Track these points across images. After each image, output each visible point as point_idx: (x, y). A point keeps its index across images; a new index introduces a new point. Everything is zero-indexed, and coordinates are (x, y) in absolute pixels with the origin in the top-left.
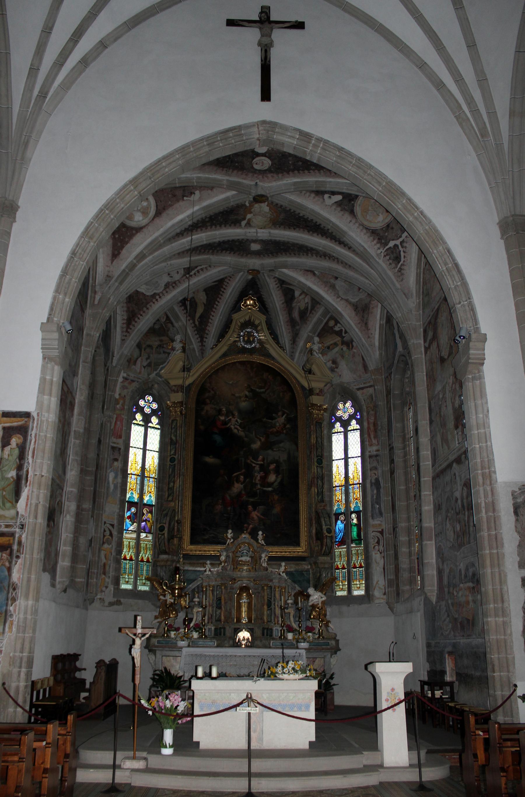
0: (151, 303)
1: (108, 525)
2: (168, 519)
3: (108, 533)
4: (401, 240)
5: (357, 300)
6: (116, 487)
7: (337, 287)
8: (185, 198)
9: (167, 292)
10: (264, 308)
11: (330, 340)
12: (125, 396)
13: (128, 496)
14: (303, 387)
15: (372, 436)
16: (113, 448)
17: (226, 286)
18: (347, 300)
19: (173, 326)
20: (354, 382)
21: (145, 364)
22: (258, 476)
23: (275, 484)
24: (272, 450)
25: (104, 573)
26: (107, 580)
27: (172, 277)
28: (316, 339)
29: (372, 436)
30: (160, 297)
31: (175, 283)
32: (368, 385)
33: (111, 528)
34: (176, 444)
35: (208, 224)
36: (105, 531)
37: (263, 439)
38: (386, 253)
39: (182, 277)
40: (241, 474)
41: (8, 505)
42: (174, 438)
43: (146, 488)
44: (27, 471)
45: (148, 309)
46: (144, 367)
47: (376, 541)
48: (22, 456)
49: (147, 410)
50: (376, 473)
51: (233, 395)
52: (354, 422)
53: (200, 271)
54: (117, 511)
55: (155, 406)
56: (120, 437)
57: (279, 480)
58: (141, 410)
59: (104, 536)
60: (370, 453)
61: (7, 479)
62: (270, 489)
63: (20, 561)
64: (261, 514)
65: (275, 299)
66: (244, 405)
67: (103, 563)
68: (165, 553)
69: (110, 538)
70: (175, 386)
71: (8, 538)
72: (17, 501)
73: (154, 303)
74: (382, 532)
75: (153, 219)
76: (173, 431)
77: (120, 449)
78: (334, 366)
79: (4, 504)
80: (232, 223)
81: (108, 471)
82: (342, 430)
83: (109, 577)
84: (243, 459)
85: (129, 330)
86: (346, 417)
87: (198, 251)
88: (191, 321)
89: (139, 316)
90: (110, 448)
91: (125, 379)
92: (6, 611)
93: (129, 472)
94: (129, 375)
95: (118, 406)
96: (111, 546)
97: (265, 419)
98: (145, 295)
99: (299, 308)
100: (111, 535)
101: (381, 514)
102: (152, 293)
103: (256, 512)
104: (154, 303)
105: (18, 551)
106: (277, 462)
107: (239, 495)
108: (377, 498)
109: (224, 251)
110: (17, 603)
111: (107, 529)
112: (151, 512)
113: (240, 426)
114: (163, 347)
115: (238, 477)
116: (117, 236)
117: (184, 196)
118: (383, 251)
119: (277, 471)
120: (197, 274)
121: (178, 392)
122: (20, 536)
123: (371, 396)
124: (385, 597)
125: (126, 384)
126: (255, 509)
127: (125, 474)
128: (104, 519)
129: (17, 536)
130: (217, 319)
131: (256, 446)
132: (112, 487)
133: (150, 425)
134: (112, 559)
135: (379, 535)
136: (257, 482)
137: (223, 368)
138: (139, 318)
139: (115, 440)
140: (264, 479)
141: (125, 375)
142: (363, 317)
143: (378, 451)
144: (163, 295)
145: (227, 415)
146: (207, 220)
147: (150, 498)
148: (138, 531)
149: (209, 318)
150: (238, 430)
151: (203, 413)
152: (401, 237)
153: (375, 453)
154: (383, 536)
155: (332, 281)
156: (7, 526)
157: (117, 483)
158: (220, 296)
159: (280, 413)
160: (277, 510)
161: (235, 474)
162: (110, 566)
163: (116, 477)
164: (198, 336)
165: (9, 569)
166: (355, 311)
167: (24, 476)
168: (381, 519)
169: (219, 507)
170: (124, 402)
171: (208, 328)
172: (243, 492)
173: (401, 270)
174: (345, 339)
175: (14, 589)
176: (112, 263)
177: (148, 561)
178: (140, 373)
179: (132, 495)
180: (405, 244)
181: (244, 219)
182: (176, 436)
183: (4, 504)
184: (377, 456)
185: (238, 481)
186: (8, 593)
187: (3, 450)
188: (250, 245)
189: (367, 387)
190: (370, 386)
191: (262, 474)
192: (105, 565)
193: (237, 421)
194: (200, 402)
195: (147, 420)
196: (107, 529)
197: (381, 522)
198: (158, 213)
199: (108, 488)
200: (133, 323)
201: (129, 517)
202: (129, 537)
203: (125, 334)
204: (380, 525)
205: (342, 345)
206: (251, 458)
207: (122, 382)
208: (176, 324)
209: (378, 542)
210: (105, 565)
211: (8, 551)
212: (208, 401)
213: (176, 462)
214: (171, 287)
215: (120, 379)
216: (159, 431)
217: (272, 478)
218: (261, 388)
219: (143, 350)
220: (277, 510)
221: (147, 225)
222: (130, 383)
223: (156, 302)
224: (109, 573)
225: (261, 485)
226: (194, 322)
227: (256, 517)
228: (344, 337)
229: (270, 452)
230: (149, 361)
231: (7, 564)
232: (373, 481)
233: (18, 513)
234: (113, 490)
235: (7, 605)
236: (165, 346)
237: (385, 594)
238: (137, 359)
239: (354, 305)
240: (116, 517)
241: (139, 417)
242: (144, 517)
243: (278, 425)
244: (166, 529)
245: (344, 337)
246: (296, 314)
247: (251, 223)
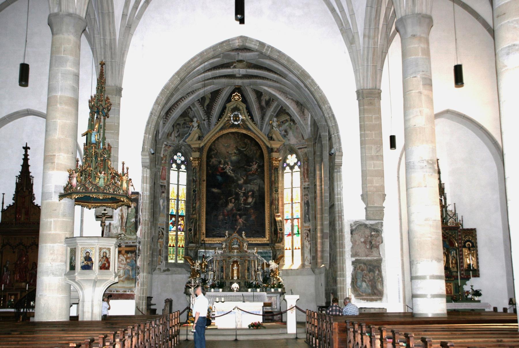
0: (180, 102)
1: (161, 229)
2: (193, 224)
3: (161, 233)
6: (164, 208)
10: (244, 100)
11: (284, 118)
13: (170, 211)
14: (267, 147)
15: (306, 176)
16: (162, 186)
19: (192, 110)
20: (296, 144)
21: (176, 135)
22: (242, 199)
23: (252, 203)
24: (250, 184)
25: (160, 255)
26: (162, 258)
28: (275, 119)
29: (306, 176)
30: (185, 99)
32: (304, 146)
33: (162, 230)
34: (196, 182)
36: (159, 232)
37: (245, 178)
40: (233, 198)
41: (133, 233)
42: (195, 178)
43: (180, 206)
44: (140, 219)
45: (178, 105)
46: (176, 137)
47: (306, 235)
48: (137, 212)
49: (179, 162)
51: (228, 152)
52: (296, 167)
54: (165, 220)
55: (183, 159)
56: (165, 179)
57: (254, 201)
58: (175, 161)
59: (159, 235)
61: (131, 222)
62: (249, 206)
63: (140, 257)
64: (245, 220)
65: (251, 97)
66: (234, 158)
68: (192, 243)
70: (194, 148)
71: (133, 248)
72: (136, 232)
74: (309, 230)
76: (194, 174)
77: (165, 186)
78: (285, 134)
79: (131, 233)
81: (160, 199)
82: (290, 171)
84: (234, 190)
85: (167, 118)
86: (292, 164)
91: (166, 145)
92: (136, 278)
93: (170, 198)
94: (168, 143)
95: (163, 162)
97: (246, 167)
99: (266, 100)
100: (163, 234)
101: (309, 220)
103: (241, 220)
105: (139, 253)
106: (253, 191)
107: (232, 210)
108: (307, 212)
110: (140, 274)
111: (160, 231)
112: (183, 220)
113: (232, 170)
114: (186, 124)
115: (231, 200)
119: (253, 196)
121: (196, 152)
122: (139, 247)
123: (306, 153)
124: (310, 265)
125: (167, 148)
126: (240, 217)
127: (168, 199)
128: (159, 226)
129: (138, 247)
130: (217, 108)
131: (241, 182)
132: (162, 207)
133: (180, 170)
135: (308, 232)
136: (242, 202)
137: (221, 136)
138: (173, 111)
139: (162, 181)
140: (245, 200)
141: (165, 143)
142: (301, 108)
143: (308, 185)
144: (186, 97)
145: (224, 165)
147: (182, 212)
148: (177, 230)
149: (213, 107)
150: (231, 173)
151: (211, 163)
153: (307, 186)
156: (133, 243)
159: (254, 163)
160: (253, 218)
161: (229, 198)
163: (164, 202)
164: (206, 116)
165: (136, 261)
166: (297, 105)
167: (139, 221)
169: (221, 217)
170: (166, 158)
171: (212, 112)
172: (234, 208)
175: (138, 269)
177: (182, 247)
178: (174, 141)
179: (173, 210)
181: (232, 65)
182: (196, 178)
183: (131, 233)
184: (308, 188)
185: (231, 202)
186: (136, 270)
187: (128, 210)
189: (304, 148)
191: (244, 198)
192: (160, 250)
193: (230, 168)
194: (209, 157)
195: (179, 167)
196: (160, 231)
199: (160, 208)
200: (170, 113)
201: (171, 223)
202: (172, 234)
203: (165, 120)
204: (309, 226)
205: (290, 121)
206: (238, 189)
208: (193, 109)
209: (307, 236)
210: (160, 250)
211: (134, 253)
212: (213, 156)
213: (196, 192)
216: (186, 173)
217: (250, 200)
218: (243, 148)
220: (253, 218)
222: (169, 148)
223: (182, 102)
225: (244, 204)
226: (204, 108)
227: (241, 222)
229: (249, 185)
230: (178, 133)
231: (134, 259)
232: (306, 202)
233: (137, 237)
235: (136, 275)
236: (187, 123)
237: (310, 263)
238: (172, 133)
239: (296, 102)
241: (174, 166)
242: (180, 223)
243: (253, 169)
244: (193, 230)
246: (263, 103)
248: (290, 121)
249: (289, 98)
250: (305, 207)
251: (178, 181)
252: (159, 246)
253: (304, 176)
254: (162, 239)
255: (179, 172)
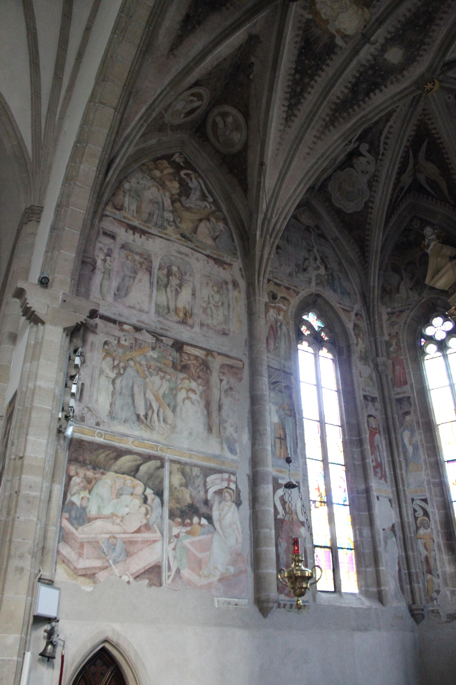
0: (369, 215)
1: (418, 502)
3: (420, 513)
6: (416, 448)
8: (251, 77)
9: (375, 192)
12: (397, 333)
16: (399, 401)
17: (437, 133)
25: (429, 571)
26: (435, 580)
27: (367, 172)
31: (375, 176)
33: (423, 504)
35: (307, 80)
36: (415, 511)
39: (376, 163)
45: (369, 224)
46: (411, 289)
53: (387, 141)
58: (431, 339)
67: (423, 557)
69: (426, 518)
70: (450, 288)
73: (371, 213)
75: (248, 126)
77: (409, 398)
80: (328, 54)
83: (438, 575)
87: (341, 119)
88: (447, 205)
89: (367, 238)
90: (394, 402)
94: (394, 308)
95: (391, 349)
96: (429, 530)
98: (358, 212)
100: (426, 514)
102: (363, 205)
104: (371, 213)
109: (372, 95)
111: (417, 508)
116: (236, 171)
117: (248, 77)
120: (387, 147)
125: (394, 319)
128: (409, 497)
132: (410, 449)
133: (449, 352)
134: (436, 548)
139: (398, 390)
141: (389, 310)
144: (373, 197)
146: (297, 76)
157: (417, 441)
158: (443, 151)
162: (435, 559)
170: (399, 340)
176: (247, 199)
178: (408, 298)
181: (333, 37)
188: (385, 60)
192: (427, 558)
198: (247, 116)
207: (388, 320)
210: (427, 558)
214: (374, 183)
215: (385, 317)
219: (403, 272)
221: (248, 136)
222: (398, 316)
224: (437, 570)
230: (415, 279)
234: (413, 453)
240: (426, 487)
241: (431, 349)
247: (347, 33)
251: (450, 377)
252: (421, 548)
254: (427, 526)
255: (445, 357)
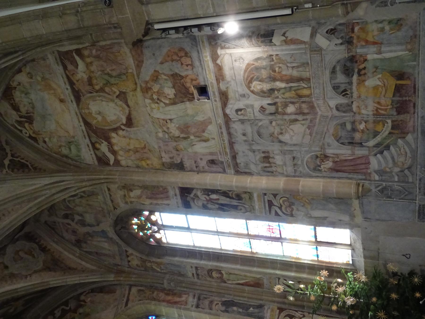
4: (9, 155)
5: (42, 265)
7: (16, 272)
15: (177, 299)
18: (35, 272)
38: (10, 170)
50: (216, 303)
60: (194, 307)
101: (261, 307)
118: (7, 170)
135: (283, 314)
143: (194, 296)
152: (7, 154)
153: (196, 300)
154: (286, 309)
155: (6, 272)
166: (50, 271)
168: (266, 307)
173: (35, 168)
174: (72, 308)
180: (16, 155)
184: (199, 299)
190: (130, 290)
197: (269, 308)
204: (272, 310)
228: (70, 308)
232: (223, 308)
245: (70, 308)
248: (76, 313)
249: (30, 275)
250: (233, 311)
253: (176, 303)
